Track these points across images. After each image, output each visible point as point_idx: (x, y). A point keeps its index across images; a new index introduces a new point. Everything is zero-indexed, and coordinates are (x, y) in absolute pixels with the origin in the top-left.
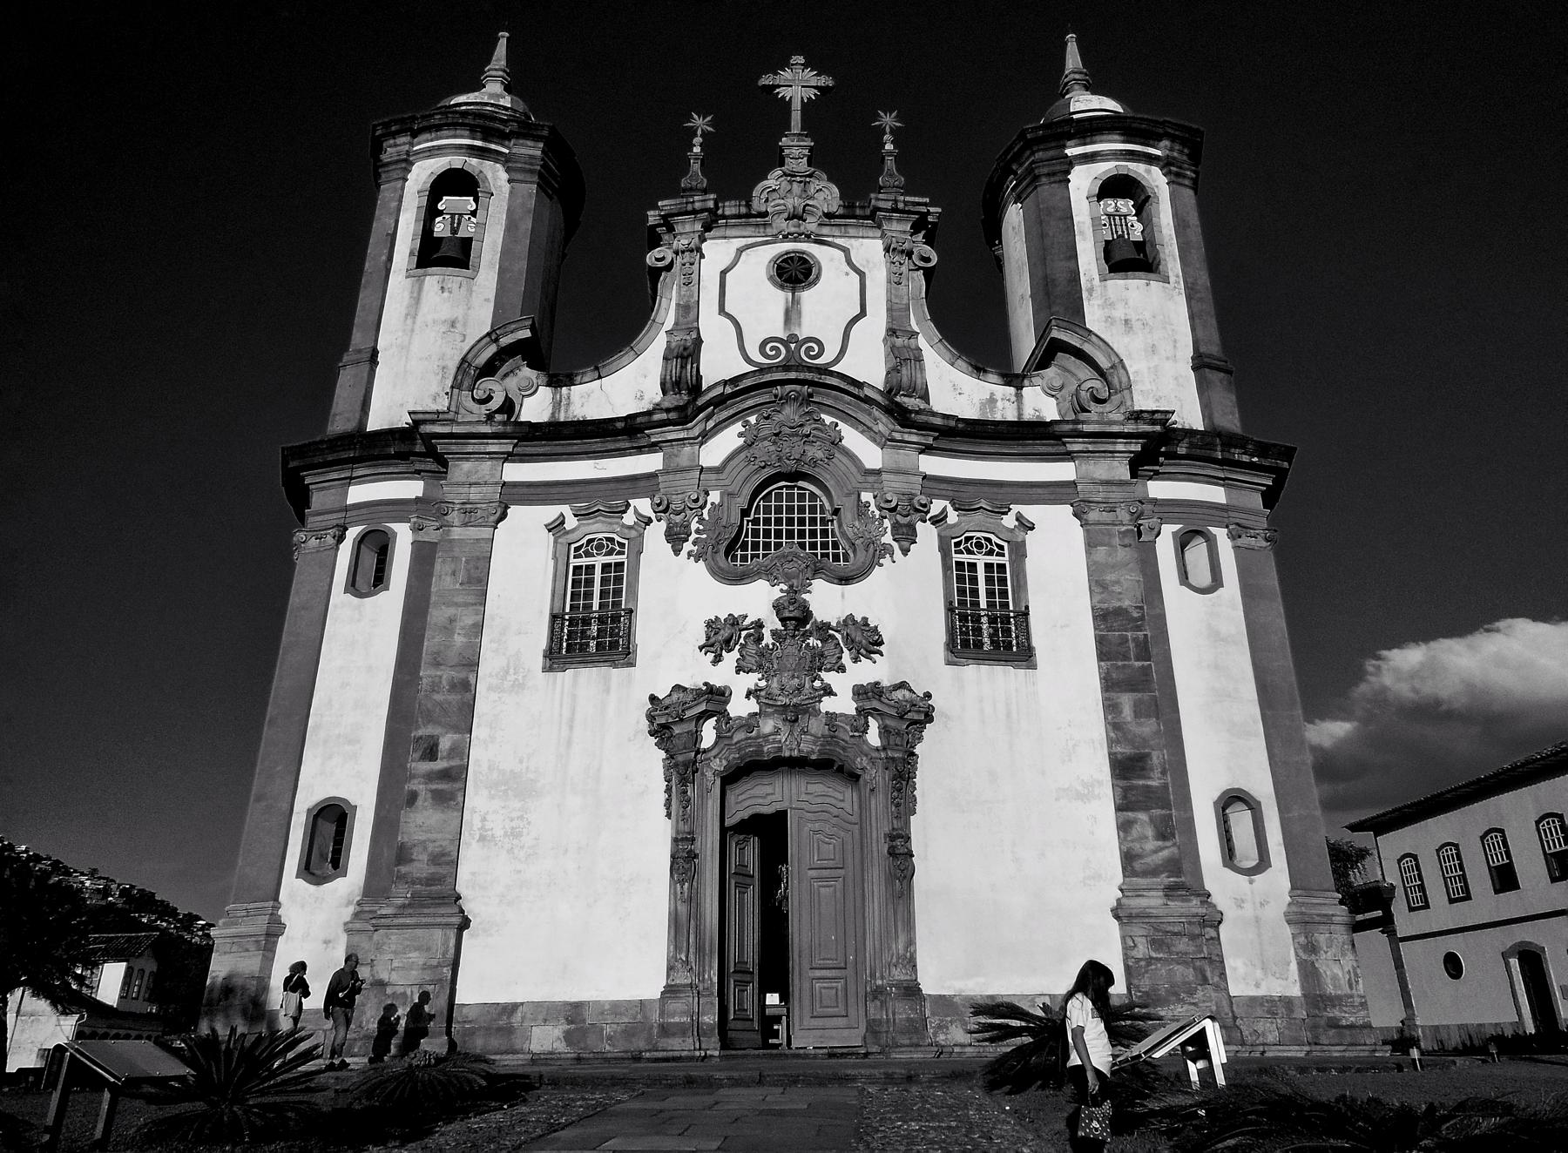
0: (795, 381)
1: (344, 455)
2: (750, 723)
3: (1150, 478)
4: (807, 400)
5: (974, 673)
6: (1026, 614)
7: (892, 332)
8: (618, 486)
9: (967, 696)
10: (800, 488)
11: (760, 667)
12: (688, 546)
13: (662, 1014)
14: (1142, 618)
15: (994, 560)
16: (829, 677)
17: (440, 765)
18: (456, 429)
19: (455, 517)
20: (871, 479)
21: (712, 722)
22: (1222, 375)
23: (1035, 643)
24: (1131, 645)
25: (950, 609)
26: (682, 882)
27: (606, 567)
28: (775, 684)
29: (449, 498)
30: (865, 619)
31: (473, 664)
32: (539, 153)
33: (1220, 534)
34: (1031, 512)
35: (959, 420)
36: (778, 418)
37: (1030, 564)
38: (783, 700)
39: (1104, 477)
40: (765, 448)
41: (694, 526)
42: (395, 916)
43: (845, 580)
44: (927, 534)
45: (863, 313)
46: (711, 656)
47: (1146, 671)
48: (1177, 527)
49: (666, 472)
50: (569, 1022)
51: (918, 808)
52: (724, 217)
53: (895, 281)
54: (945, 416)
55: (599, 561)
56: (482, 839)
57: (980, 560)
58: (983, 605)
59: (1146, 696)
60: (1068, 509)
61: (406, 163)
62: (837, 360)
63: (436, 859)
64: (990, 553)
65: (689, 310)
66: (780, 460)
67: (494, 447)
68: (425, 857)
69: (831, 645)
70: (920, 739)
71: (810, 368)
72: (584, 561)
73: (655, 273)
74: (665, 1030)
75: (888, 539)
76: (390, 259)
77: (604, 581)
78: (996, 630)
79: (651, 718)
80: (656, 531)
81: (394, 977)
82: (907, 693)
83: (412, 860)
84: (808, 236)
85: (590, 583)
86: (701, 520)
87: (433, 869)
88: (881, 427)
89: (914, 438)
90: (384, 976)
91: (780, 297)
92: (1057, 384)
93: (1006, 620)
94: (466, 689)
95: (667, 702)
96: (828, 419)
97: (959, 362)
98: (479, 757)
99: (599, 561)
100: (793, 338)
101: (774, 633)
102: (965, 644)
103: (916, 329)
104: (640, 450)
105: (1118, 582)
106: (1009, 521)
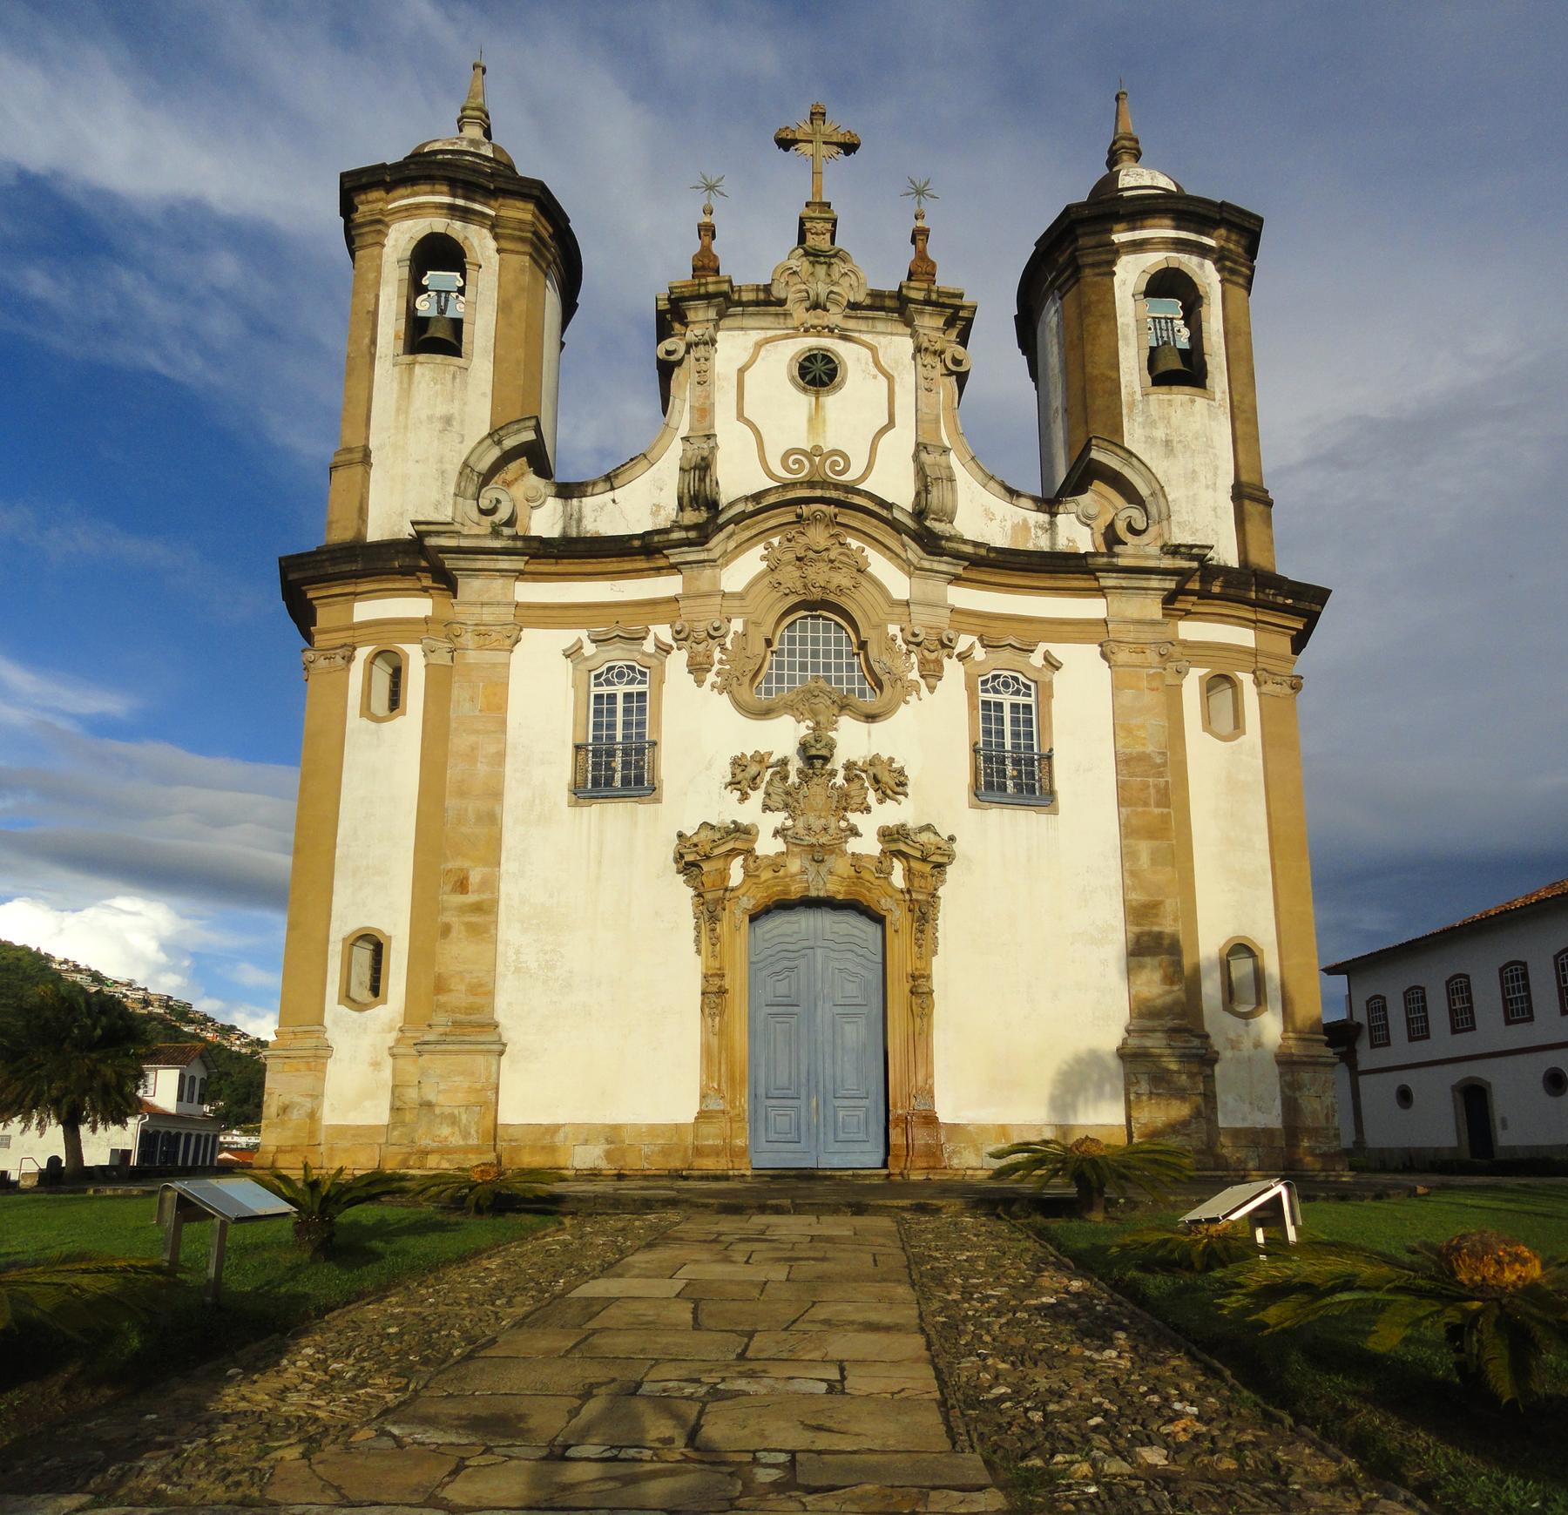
0: (818, 500)
1: (346, 568)
2: (776, 863)
3: (1181, 618)
4: (833, 522)
5: (999, 818)
6: (1049, 758)
7: (921, 447)
8: (637, 610)
9: (989, 841)
10: (825, 618)
11: (787, 806)
12: (711, 677)
13: (696, 1137)
14: (1164, 764)
15: (1021, 700)
16: (855, 818)
17: (471, 898)
18: (464, 543)
19: (468, 639)
20: (899, 610)
21: (739, 861)
22: (1261, 507)
23: (1058, 785)
24: (1152, 791)
25: (976, 751)
26: (712, 1016)
27: (628, 696)
28: (800, 824)
29: (462, 618)
30: (892, 760)
31: (497, 795)
32: (529, 217)
33: (1246, 679)
34: (1059, 651)
35: (990, 549)
36: (802, 540)
37: (1057, 706)
38: (813, 840)
39: (1136, 615)
40: (790, 575)
41: (717, 655)
42: (437, 1043)
43: (871, 718)
44: (953, 671)
45: (891, 423)
46: (737, 794)
47: (1165, 819)
48: (1204, 671)
49: (686, 596)
50: (609, 1142)
51: (940, 948)
52: (740, 303)
53: (924, 387)
54: (976, 544)
55: (620, 689)
56: (518, 970)
57: (1007, 699)
58: (1008, 747)
59: (1164, 844)
60: (1096, 649)
61: (380, 224)
62: (864, 477)
63: (474, 989)
64: (1017, 692)
65: (704, 412)
66: (805, 586)
67: (505, 563)
68: (463, 988)
69: (856, 785)
70: (943, 882)
71: (836, 486)
72: (605, 690)
73: (666, 369)
74: (699, 1151)
75: (914, 675)
76: (374, 342)
77: (627, 711)
78: (1020, 772)
79: (680, 856)
80: (678, 661)
81: (441, 1099)
82: (932, 836)
83: (450, 991)
84: (831, 331)
85: (612, 712)
86: (723, 648)
87: (471, 999)
88: (911, 555)
89: (944, 568)
90: (432, 1097)
91: (802, 402)
92: (1092, 512)
93: (1031, 762)
94: (492, 820)
95: (695, 840)
96: (854, 543)
97: (992, 484)
98: (510, 891)
99: (620, 689)
100: (817, 448)
101: (800, 772)
102: (989, 785)
103: (947, 444)
104: (658, 571)
105: (1143, 727)
106: (1037, 659)
